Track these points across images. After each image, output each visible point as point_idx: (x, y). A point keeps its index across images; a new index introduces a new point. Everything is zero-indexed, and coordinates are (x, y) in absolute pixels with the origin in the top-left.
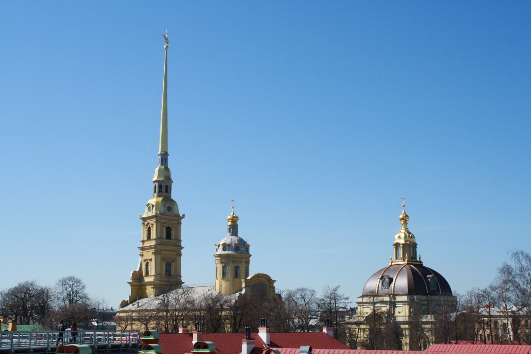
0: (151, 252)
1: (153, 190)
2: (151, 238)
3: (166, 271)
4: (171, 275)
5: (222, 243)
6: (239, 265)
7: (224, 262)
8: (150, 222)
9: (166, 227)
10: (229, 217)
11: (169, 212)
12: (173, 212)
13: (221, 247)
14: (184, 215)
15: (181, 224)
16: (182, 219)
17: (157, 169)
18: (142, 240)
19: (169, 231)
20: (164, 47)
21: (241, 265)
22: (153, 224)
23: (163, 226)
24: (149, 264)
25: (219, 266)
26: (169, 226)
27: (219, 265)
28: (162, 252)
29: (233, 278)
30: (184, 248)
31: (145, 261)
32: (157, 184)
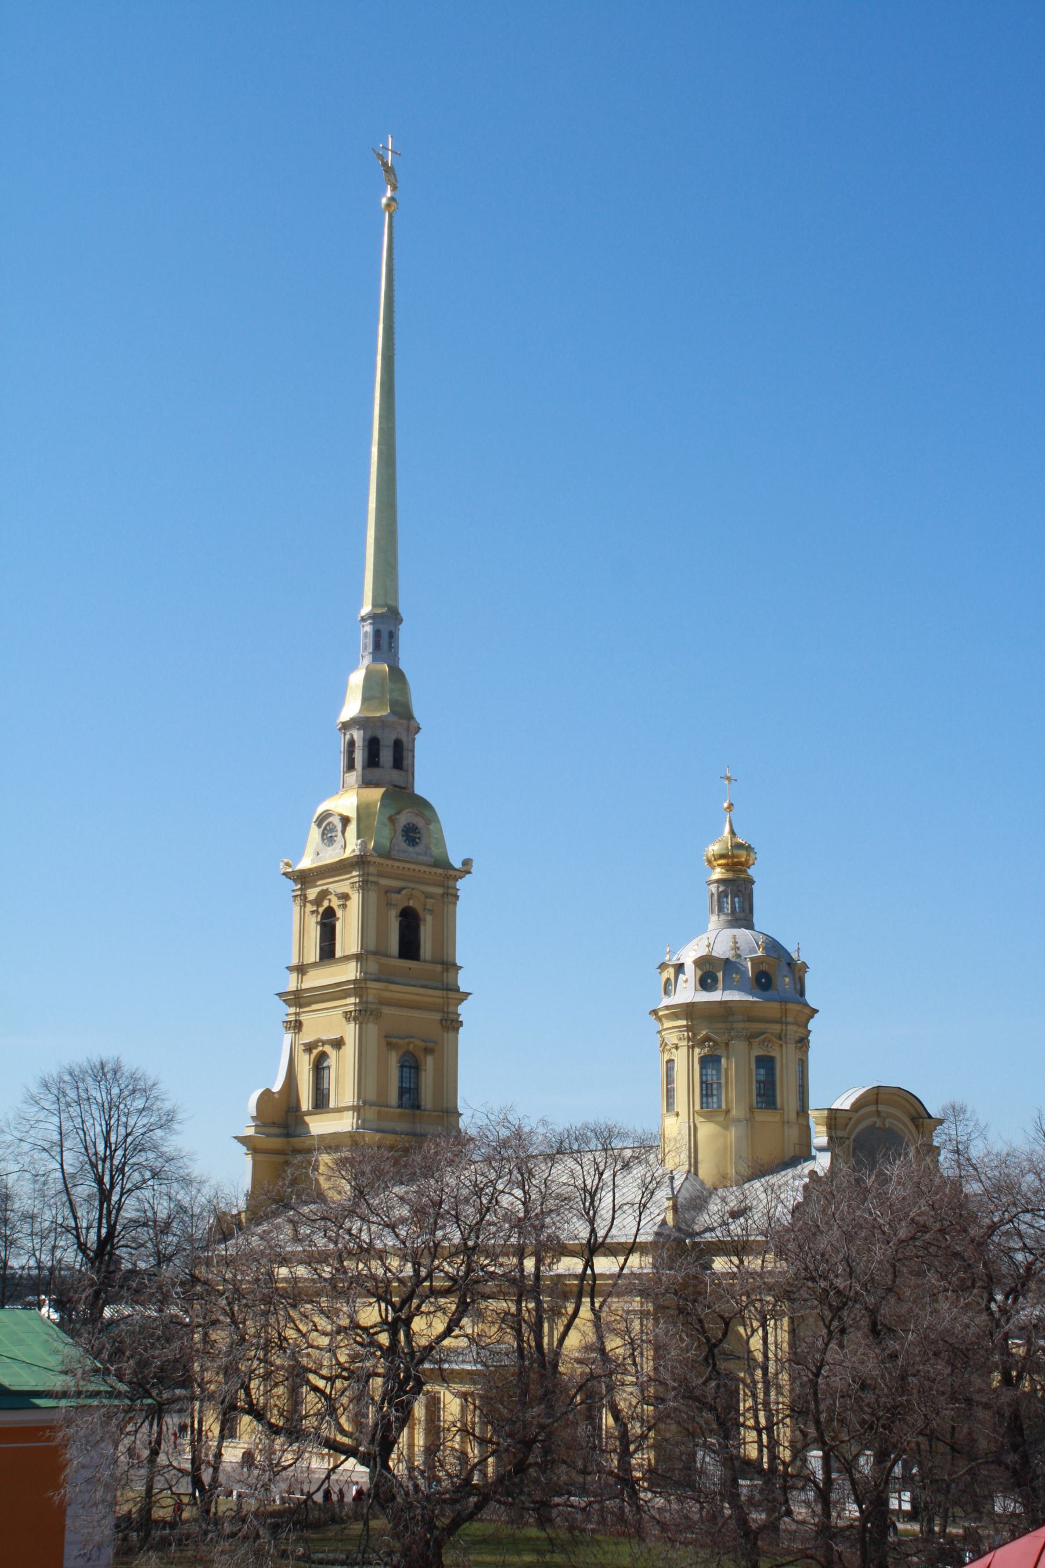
0: (339, 1012)
1: (342, 761)
2: (338, 954)
3: (402, 1091)
4: (419, 1107)
5: (689, 956)
6: (772, 1054)
7: (707, 1039)
8: (331, 888)
9: (399, 910)
10: (715, 848)
11: (411, 849)
12: (428, 848)
13: (690, 972)
14: (467, 863)
15: (457, 897)
16: (461, 878)
17: (357, 679)
18: (295, 962)
19: (410, 922)
20: (380, 203)
21: (781, 1051)
22: (345, 897)
23: (389, 905)
24: (332, 1061)
25: (680, 1058)
26: (411, 904)
27: (683, 1051)
28: (386, 1010)
29: (751, 1109)
30: (470, 997)
31: (309, 1048)
32: (357, 735)
